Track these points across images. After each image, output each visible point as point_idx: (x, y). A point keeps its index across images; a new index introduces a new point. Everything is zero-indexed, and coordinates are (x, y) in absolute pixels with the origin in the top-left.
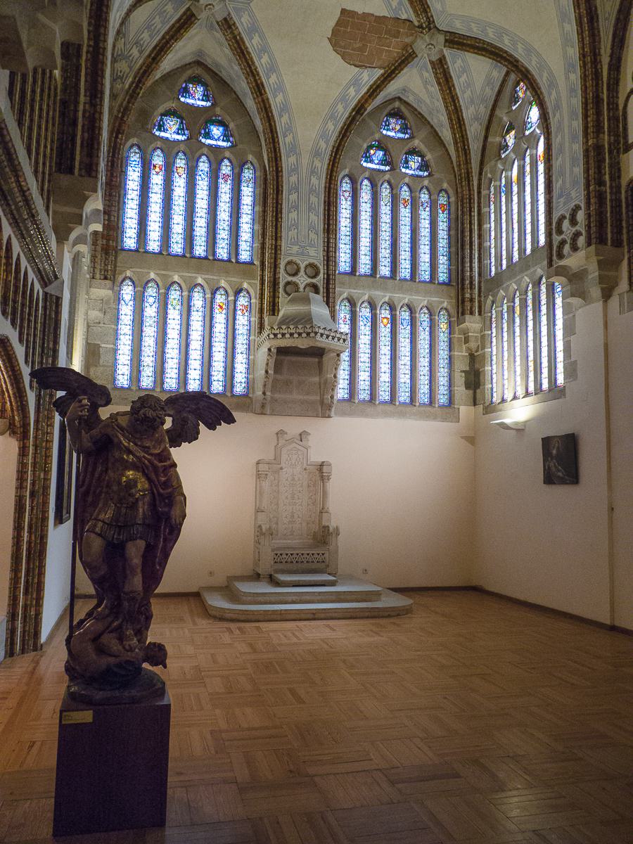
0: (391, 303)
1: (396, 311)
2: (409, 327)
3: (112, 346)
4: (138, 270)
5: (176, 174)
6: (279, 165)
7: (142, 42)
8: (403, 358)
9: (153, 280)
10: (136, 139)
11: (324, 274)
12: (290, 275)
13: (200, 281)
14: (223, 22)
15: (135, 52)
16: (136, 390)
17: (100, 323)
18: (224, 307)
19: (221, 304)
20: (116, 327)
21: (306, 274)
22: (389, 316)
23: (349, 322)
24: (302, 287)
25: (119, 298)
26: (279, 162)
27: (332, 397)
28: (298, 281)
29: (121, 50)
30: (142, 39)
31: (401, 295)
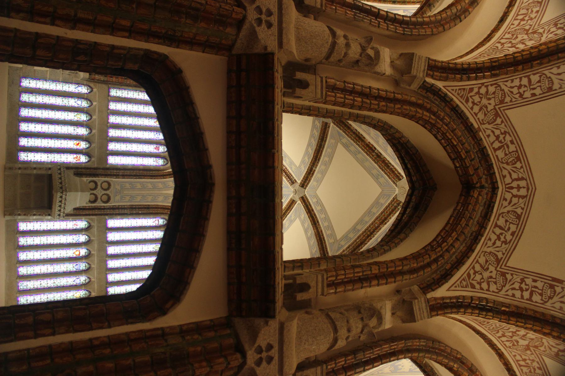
0: (90, 255)
1: (85, 259)
2: (75, 270)
3: (48, 77)
4: (97, 96)
6: (167, 177)
8: (52, 267)
9: (92, 104)
11: (104, 206)
12: (101, 184)
13: (94, 131)
16: (19, 90)
18: (78, 146)
19: (80, 145)
21: (103, 195)
22: (81, 255)
23: (75, 228)
24: (94, 192)
25: (79, 84)
26: (169, 176)
27: (19, 215)
28: (98, 189)
31: (96, 262)
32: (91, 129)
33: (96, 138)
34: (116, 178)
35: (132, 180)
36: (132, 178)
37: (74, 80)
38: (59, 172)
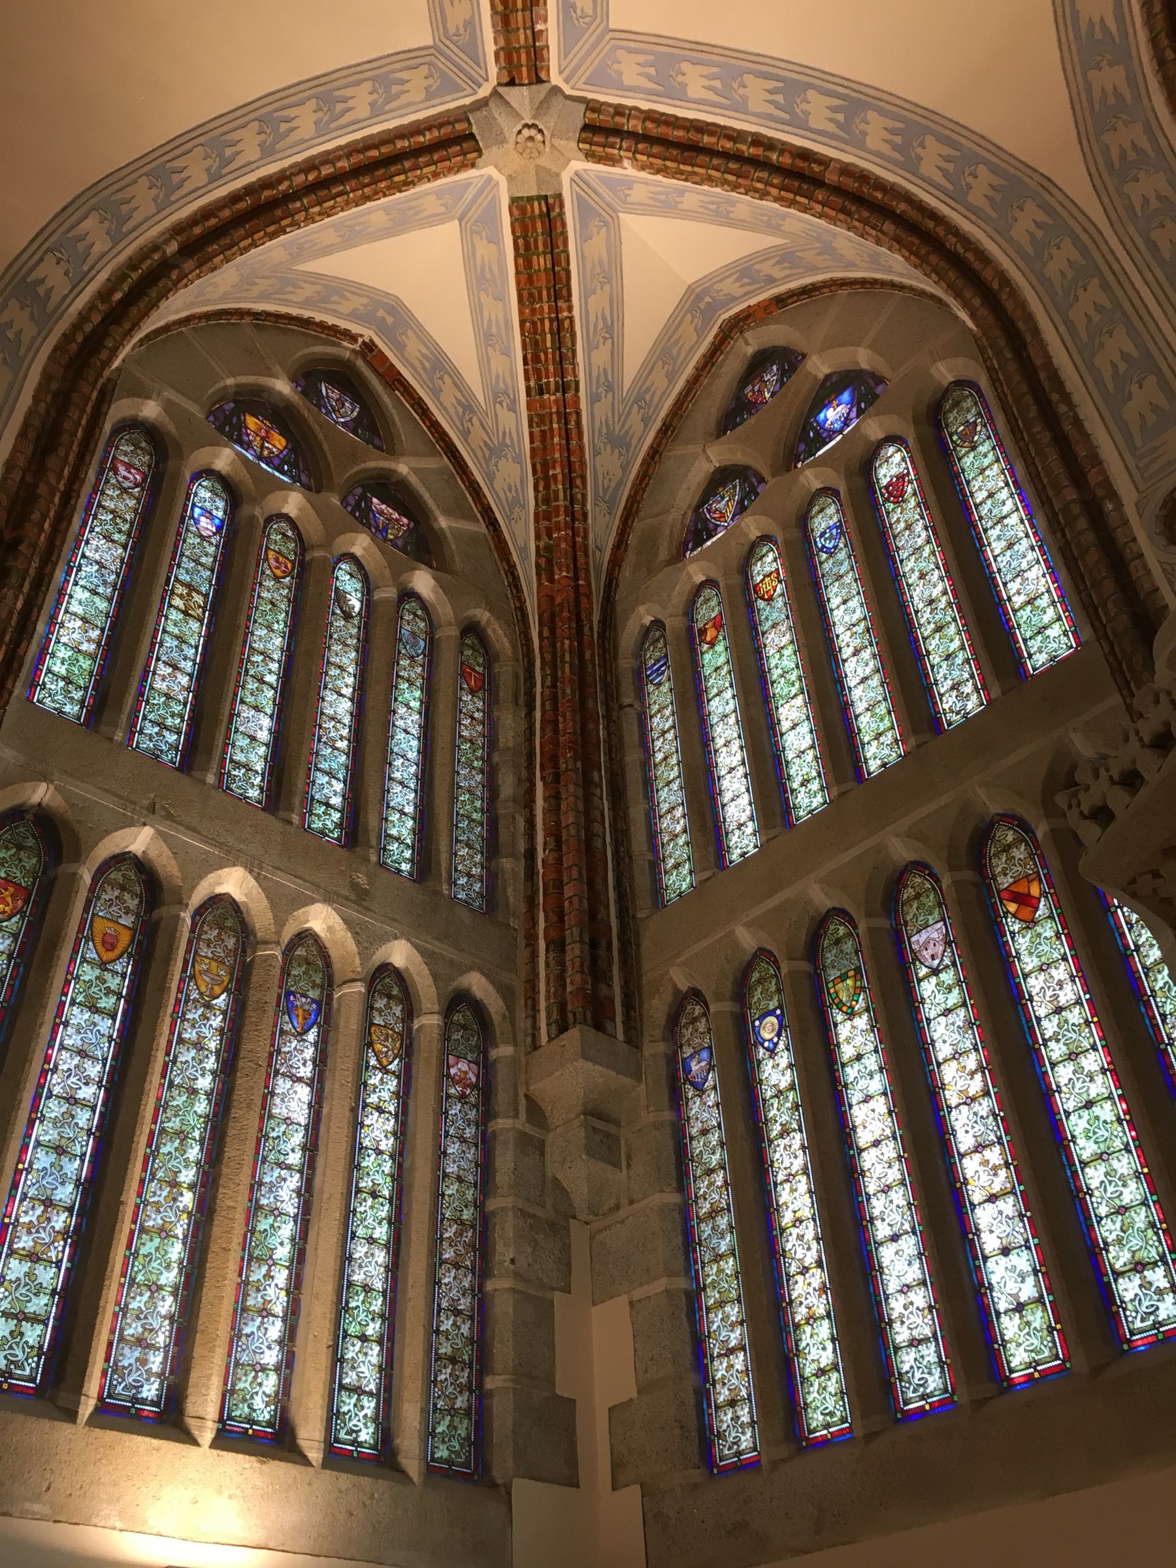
3: (661, 1284)
4: (703, 944)
5: (759, 601)
7: (501, 385)
10: (642, 609)
13: (902, 851)
14: (584, 135)
15: (507, 419)
17: (618, 1207)
18: (1035, 890)
19: (1021, 889)
20: (675, 1198)
29: (486, 444)
30: (498, 377)
32: (899, 879)
33: (932, 807)
34: (1113, 495)
35: (1088, 412)
36: (1077, 422)
37: (651, 1118)
38: (1118, 799)
